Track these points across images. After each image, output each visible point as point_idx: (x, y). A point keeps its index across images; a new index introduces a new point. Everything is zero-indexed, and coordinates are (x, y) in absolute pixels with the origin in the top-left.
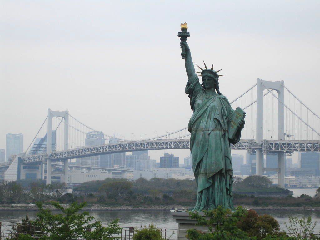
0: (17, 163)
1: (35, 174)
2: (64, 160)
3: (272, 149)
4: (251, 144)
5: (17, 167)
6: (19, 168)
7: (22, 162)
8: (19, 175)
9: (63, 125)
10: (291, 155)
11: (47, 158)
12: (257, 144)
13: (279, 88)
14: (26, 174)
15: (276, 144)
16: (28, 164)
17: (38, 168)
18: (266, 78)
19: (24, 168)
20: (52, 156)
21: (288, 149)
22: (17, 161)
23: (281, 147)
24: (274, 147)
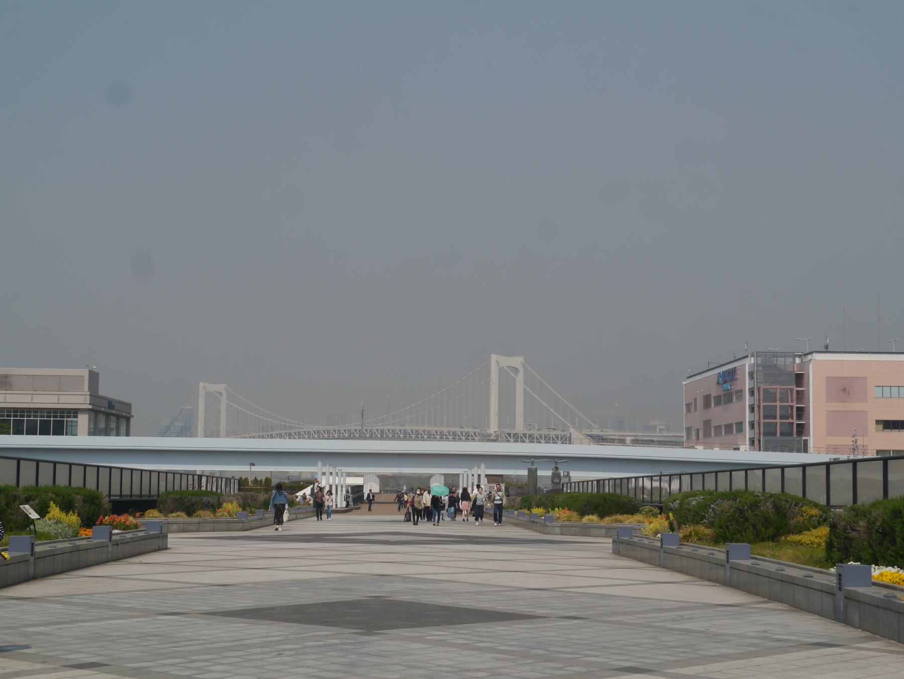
12: (491, 434)
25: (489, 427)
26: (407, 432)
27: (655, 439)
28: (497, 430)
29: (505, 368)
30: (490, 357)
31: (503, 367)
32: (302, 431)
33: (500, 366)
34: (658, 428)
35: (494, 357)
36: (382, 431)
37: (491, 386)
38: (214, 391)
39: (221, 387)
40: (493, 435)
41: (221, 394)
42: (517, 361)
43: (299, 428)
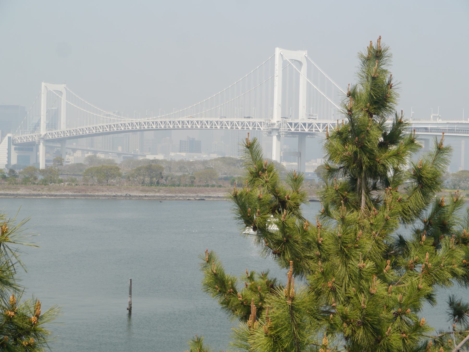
0: (7, 144)
2: (61, 141)
3: (291, 130)
4: (267, 123)
5: (7, 148)
6: (9, 150)
7: (13, 143)
8: (9, 158)
10: (313, 137)
11: (41, 138)
12: (274, 124)
14: (18, 156)
16: (19, 145)
17: (32, 150)
19: (15, 149)
20: (47, 136)
21: (309, 130)
22: (7, 142)
23: (301, 128)
24: (293, 127)
25: (272, 118)
26: (193, 123)
27: (429, 126)
28: (280, 120)
29: (288, 60)
30: (274, 51)
31: (286, 60)
32: (119, 123)
33: (284, 59)
34: (432, 117)
35: (278, 51)
36: (183, 122)
37: (275, 77)
38: (54, 91)
39: (61, 87)
40: (276, 124)
41: (61, 93)
42: (301, 55)
43: (118, 121)
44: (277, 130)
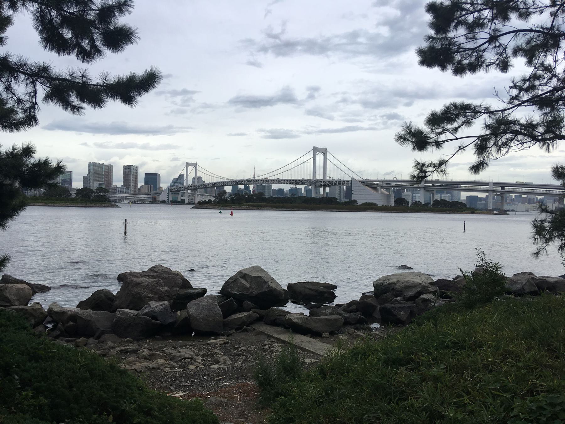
1: (177, 197)
6: (168, 194)
9: (194, 169)
13: (324, 152)
14: (172, 197)
15: (324, 182)
16: (173, 191)
17: (179, 194)
18: (318, 146)
44: (314, 184)
